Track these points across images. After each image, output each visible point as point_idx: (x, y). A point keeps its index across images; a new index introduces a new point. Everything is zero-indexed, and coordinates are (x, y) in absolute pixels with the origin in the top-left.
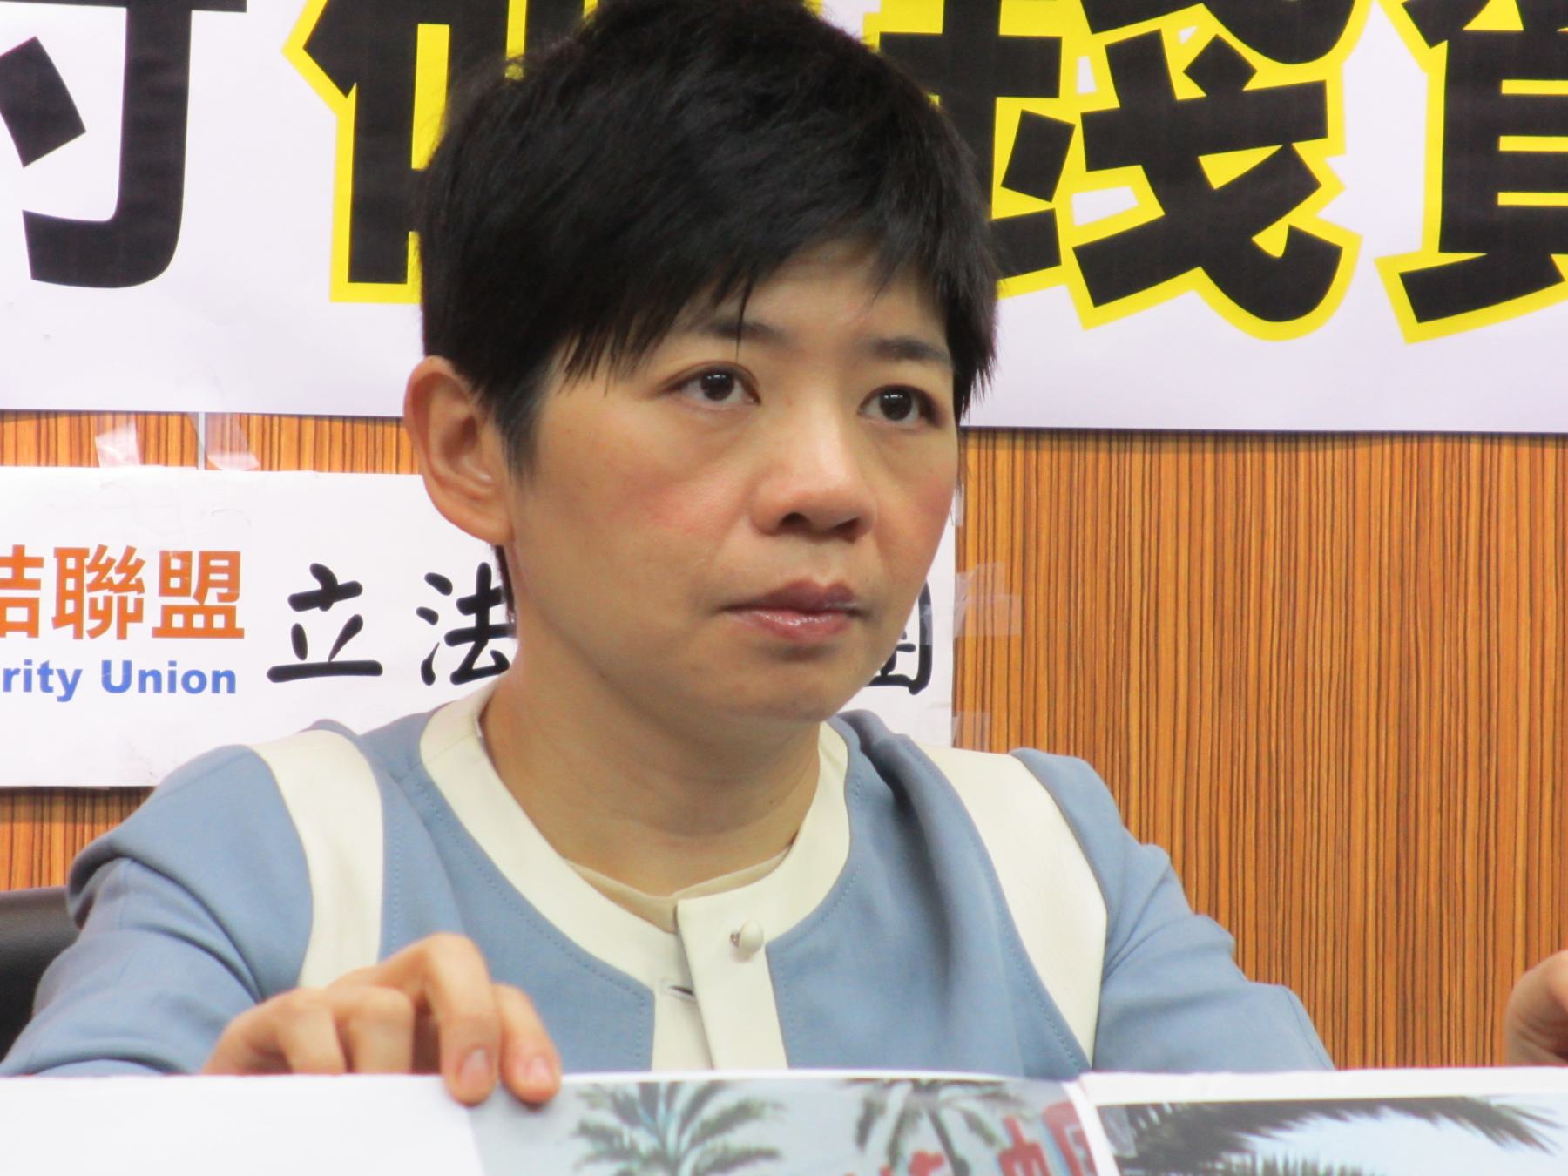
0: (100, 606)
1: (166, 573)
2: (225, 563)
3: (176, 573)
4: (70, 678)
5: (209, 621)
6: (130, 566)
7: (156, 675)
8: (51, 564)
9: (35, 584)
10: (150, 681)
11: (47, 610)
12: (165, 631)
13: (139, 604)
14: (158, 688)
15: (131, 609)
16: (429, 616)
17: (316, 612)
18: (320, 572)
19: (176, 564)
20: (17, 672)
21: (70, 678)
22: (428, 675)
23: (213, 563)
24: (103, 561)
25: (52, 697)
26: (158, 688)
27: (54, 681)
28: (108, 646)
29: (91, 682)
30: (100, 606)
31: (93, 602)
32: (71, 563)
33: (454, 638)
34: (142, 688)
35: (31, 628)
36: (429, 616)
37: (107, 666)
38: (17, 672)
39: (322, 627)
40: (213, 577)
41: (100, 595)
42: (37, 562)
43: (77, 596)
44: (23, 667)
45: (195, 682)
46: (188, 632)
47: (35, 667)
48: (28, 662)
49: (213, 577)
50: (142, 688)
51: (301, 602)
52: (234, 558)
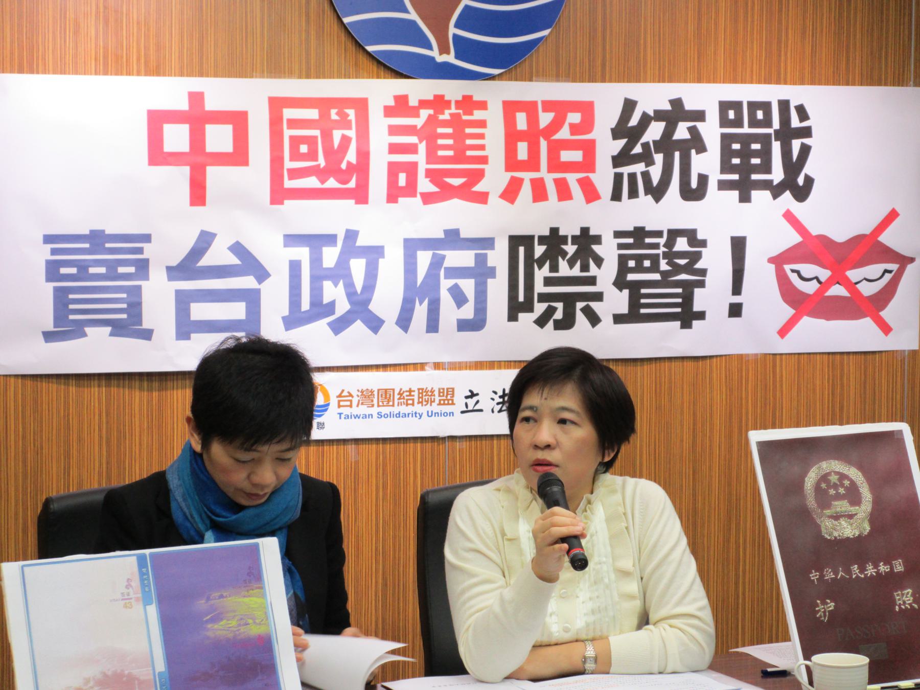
1: (440, 392)
6: (432, 391)
11: (416, 401)
12: (440, 404)
16: (493, 399)
18: (471, 391)
22: (493, 411)
29: (425, 414)
33: (498, 404)
35: (413, 404)
36: (493, 399)
39: (471, 402)
45: (445, 414)
46: (444, 404)
51: (467, 397)
52: (453, 389)
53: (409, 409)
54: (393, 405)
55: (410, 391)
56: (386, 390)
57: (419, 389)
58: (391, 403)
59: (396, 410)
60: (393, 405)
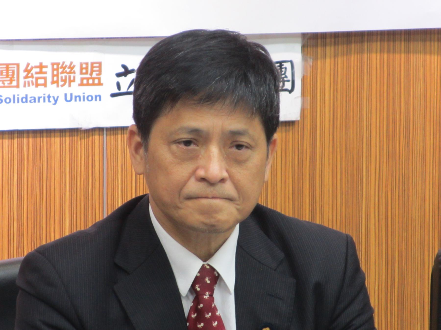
0: (64, 78)
1: (81, 68)
2: (98, 65)
3: (84, 68)
4: (56, 98)
5: (93, 81)
6: (72, 67)
7: (80, 97)
8: (50, 67)
9: (46, 73)
10: (78, 98)
11: (49, 80)
12: (81, 84)
13: (74, 77)
14: (80, 100)
15: (72, 79)
17: (123, 77)
19: (84, 66)
20: (41, 97)
21: (56, 98)
23: (95, 65)
24: (64, 66)
25: (51, 104)
26: (80, 100)
27: (52, 99)
28: (66, 89)
29: (61, 100)
30: (64, 78)
31: (62, 77)
32: (55, 67)
34: (76, 100)
35: (45, 85)
37: (66, 95)
38: (41, 97)
40: (95, 69)
41: (64, 75)
42: (46, 67)
43: (57, 75)
44: (43, 96)
45: (90, 98)
46: (88, 84)
47: (46, 96)
48: (44, 94)
49: (95, 69)
50: (76, 100)
52: (100, 63)
53: (40, 91)
54: (18, 86)
55: (41, 66)
56: (7, 65)
57: (53, 64)
58: (14, 83)
59: (21, 92)
60: (18, 86)
